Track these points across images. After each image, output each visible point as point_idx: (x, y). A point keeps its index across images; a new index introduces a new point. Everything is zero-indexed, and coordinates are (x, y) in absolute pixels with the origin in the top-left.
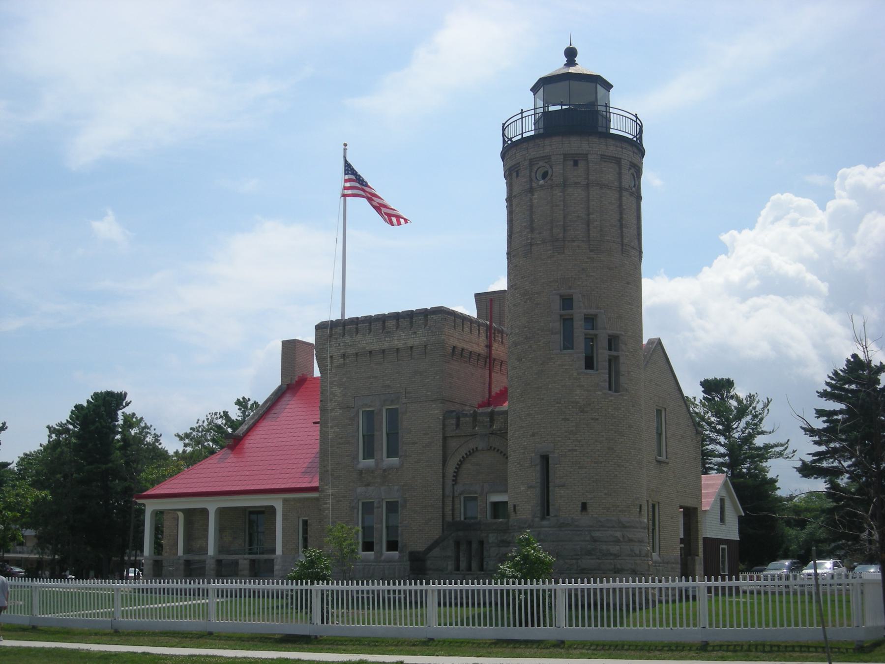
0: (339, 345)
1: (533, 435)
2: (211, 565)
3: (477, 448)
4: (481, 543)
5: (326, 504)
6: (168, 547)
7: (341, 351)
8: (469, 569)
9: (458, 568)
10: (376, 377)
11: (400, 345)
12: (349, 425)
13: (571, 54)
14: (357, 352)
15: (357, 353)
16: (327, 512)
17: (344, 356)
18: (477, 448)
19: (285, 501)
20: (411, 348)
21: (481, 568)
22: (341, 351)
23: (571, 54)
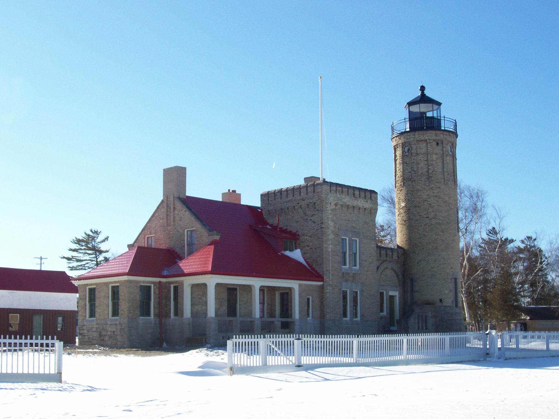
0: (335, 198)
1: (451, 268)
2: (258, 324)
3: (387, 267)
4: (426, 317)
5: (327, 289)
6: (132, 309)
7: (336, 201)
8: (422, 329)
9: (419, 329)
10: (349, 221)
11: (361, 206)
12: (338, 245)
13: (423, 88)
14: (343, 204)
15: (342, 205)
16: (328, 294)
17: (336, 205)
18: (387, 267)
19: (300, 285)
20: (365, 209)
21: (426, 329)
22: (336, 201)
23: (423, 88)
